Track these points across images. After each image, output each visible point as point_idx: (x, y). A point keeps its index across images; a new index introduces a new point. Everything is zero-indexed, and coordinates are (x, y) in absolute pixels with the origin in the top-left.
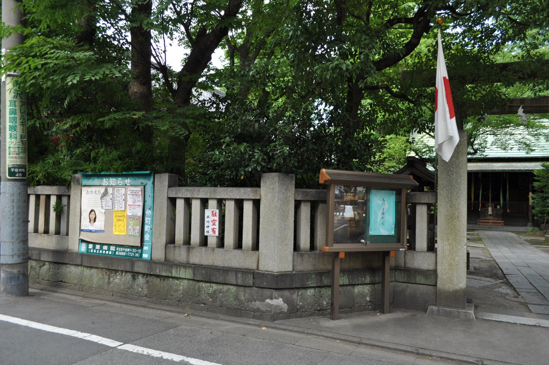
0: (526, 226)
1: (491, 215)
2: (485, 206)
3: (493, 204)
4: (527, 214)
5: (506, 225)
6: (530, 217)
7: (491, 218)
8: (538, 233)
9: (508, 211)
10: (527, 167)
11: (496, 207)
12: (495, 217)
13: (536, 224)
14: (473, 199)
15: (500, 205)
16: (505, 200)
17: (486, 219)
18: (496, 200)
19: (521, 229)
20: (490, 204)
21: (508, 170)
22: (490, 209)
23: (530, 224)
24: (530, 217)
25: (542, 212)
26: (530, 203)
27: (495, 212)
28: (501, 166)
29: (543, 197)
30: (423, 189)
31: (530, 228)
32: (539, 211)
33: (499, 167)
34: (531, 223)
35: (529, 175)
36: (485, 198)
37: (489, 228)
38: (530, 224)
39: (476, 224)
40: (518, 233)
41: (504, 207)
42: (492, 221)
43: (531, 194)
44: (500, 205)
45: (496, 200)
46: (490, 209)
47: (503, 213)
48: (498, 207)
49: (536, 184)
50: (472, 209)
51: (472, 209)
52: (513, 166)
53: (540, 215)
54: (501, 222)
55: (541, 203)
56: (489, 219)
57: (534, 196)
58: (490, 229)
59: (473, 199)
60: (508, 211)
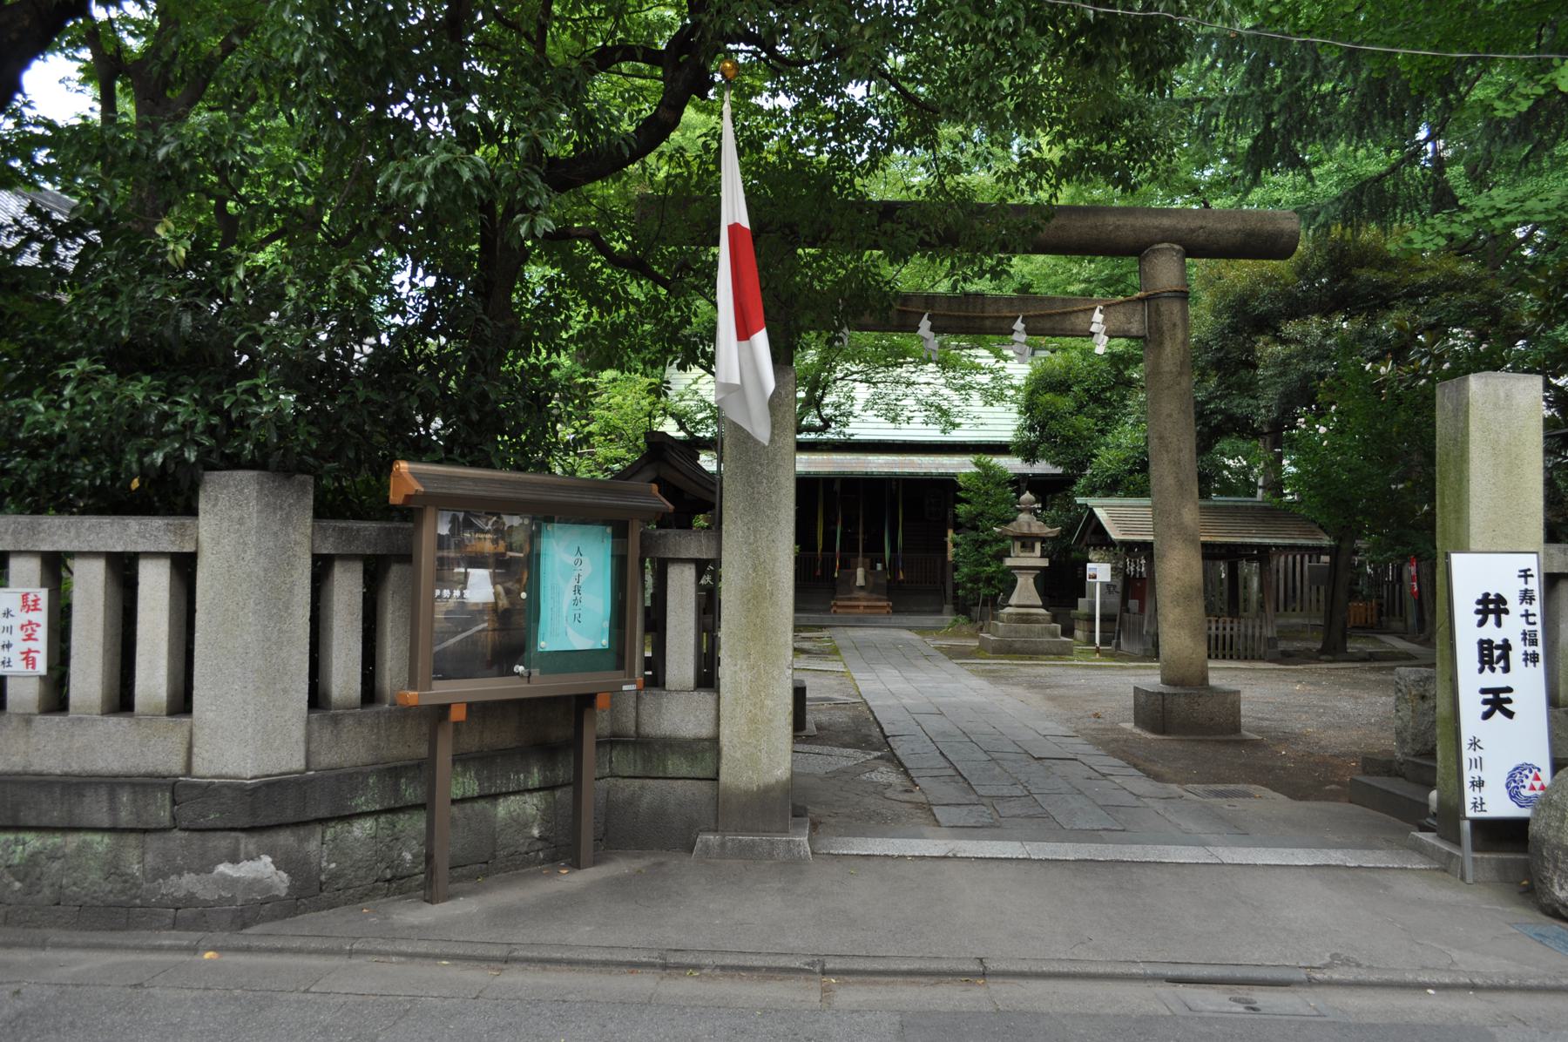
0: (940, 612)
1: (861, 588)
2: (848, 566)
4: (944, 583)
5: (896, 611)
6: (950, 591)
7: (862, 594)
8: (964, 629)
9: (901, 576)
10: (943, 466)
12: (872, 592)
13: (962, 608)
14: (820, 547)
15: (882, 561)
19: (929, 621)
20: (860, 559)
21: (903, 474)
22: (860, 572)
23: (948, 607)
24: (950, 591)
25: (975, 579)
26: (950, 558)
27: (871, 579)
28: (809, 463)
31: (948, 618)
33: (881, 465)
35: (945, 486)
36: (850, 545)
37: (859, 620)
38: (948, 607)
39: (827, 611)
40: (922, 631)
41: (893, 568)
43: (950, 533)
44: (882, 561)
45: (873, 548)
46: (860, 572)
48: (879, 567)
49: (962, 509)
52: (912, 463)
55: (974, 557)
57: (958, 538)
58: (860, 623)
59: (820, 547)
60: (901, 576)
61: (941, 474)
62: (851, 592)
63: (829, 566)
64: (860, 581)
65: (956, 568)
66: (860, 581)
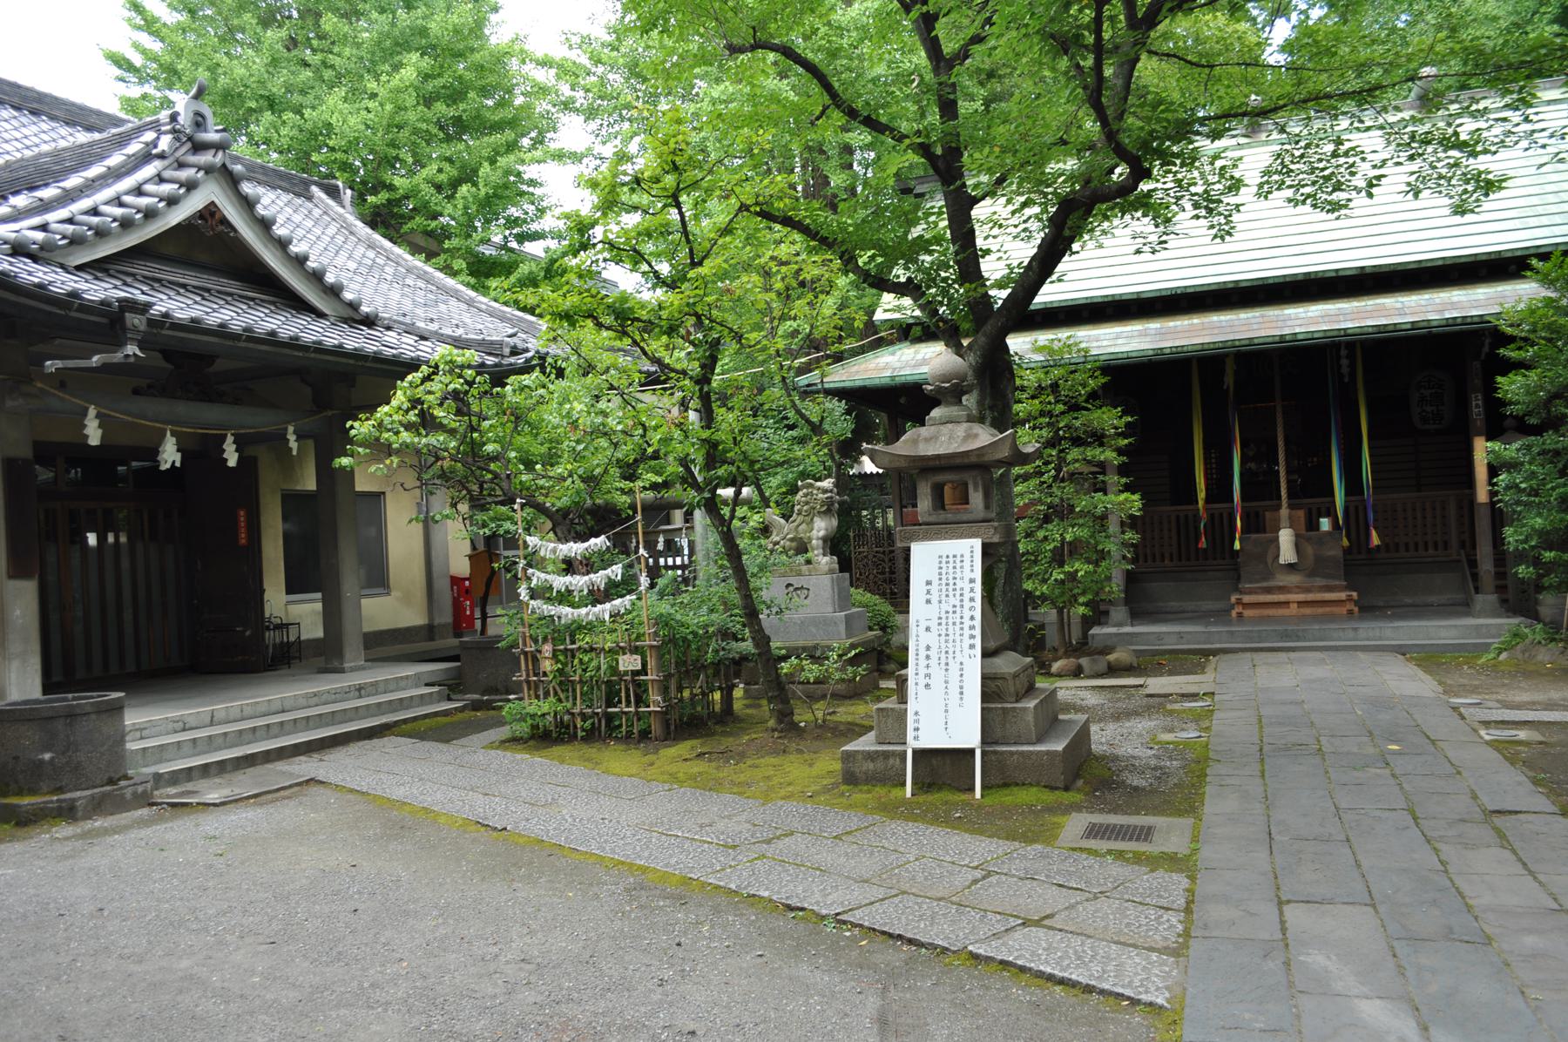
0: (1463, 607)
1: (1291, 567)
2: (1258, 524)
3: (1301, 514)
5: (1367, 609)
6: (1486, 566)
7: (1293, 579)
8: (1546, 656)
9: (1375, 540)
10: (1454, 306)
11: (1313, 525)
12: (1312, 574)
13: (1519, 601)
14: (1202, 495)
15: (1330, 512)
16: (1354, 485)
17: (1268, 590)
18: (1311, 491)
20: (1284, 512)
21: (1362, 331)
22: (1286, 537)
24: (1486, 566)
26: (1482, 495)
27: (1309, 550)
29: (1557, 453)
30: (342, 469)
31: (1487, 626)
32: (1541, 533)
34: (1493, 598)
35: (1477, 346)
36: (1260, 488)
37: (1285, 636)
38: (1487, 599)
39: (1222, 615)
40: (1429, 658)
41: (1355, 523)
42: (1301, 597)
43: (1482, 450)
44: (1330, 512)
45: (1311, 491)
46: (1286, 537)
47: (1347, 551)
48: (1325, 524)
49: (1511, 386)
50: (1203, 543)
51: (1203, 543)
52: (1384, 308)
53: (1549, 555)
54: (1343, 595)
56: (1282, 589)
57: (1511, 450)
58: (1287, 640)
59: (1202, 495)
60: (1375, 540)
61: (1453, 322)
62: (1268, 575)
63: (1221, 529)
64: (1287, 554)
65: (1499, 518)
66: (1287, 554)
